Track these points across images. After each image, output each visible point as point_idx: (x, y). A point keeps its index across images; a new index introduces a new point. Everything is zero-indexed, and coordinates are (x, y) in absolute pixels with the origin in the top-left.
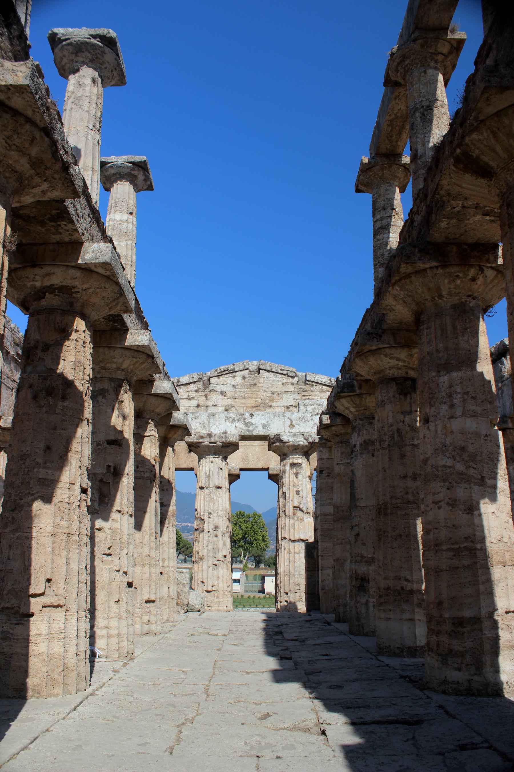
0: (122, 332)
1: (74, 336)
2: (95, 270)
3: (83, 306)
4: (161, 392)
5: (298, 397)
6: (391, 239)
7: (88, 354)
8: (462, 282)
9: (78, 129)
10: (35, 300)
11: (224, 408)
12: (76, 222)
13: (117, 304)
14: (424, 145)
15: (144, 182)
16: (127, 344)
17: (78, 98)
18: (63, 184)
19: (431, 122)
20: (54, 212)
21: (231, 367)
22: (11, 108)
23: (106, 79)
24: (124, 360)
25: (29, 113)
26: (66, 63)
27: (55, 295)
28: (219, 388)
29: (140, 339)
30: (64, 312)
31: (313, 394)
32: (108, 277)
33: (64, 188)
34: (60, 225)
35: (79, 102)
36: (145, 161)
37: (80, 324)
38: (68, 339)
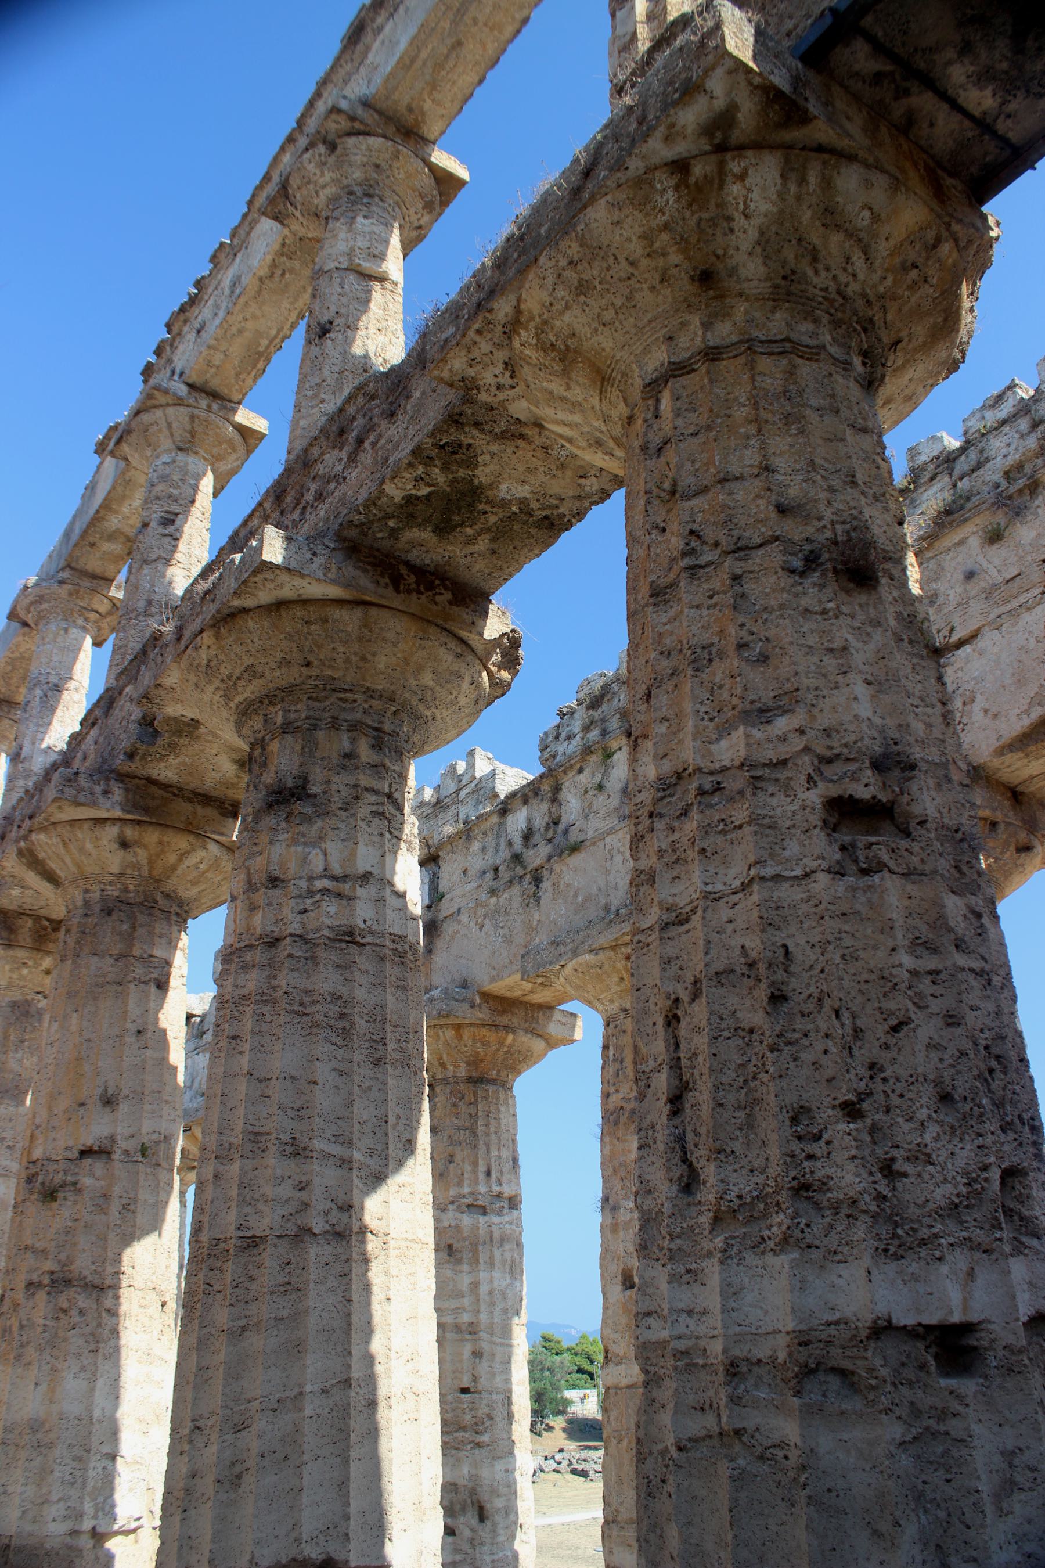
8: (30, 972)
14: (33, 743)
19: (53, 710)
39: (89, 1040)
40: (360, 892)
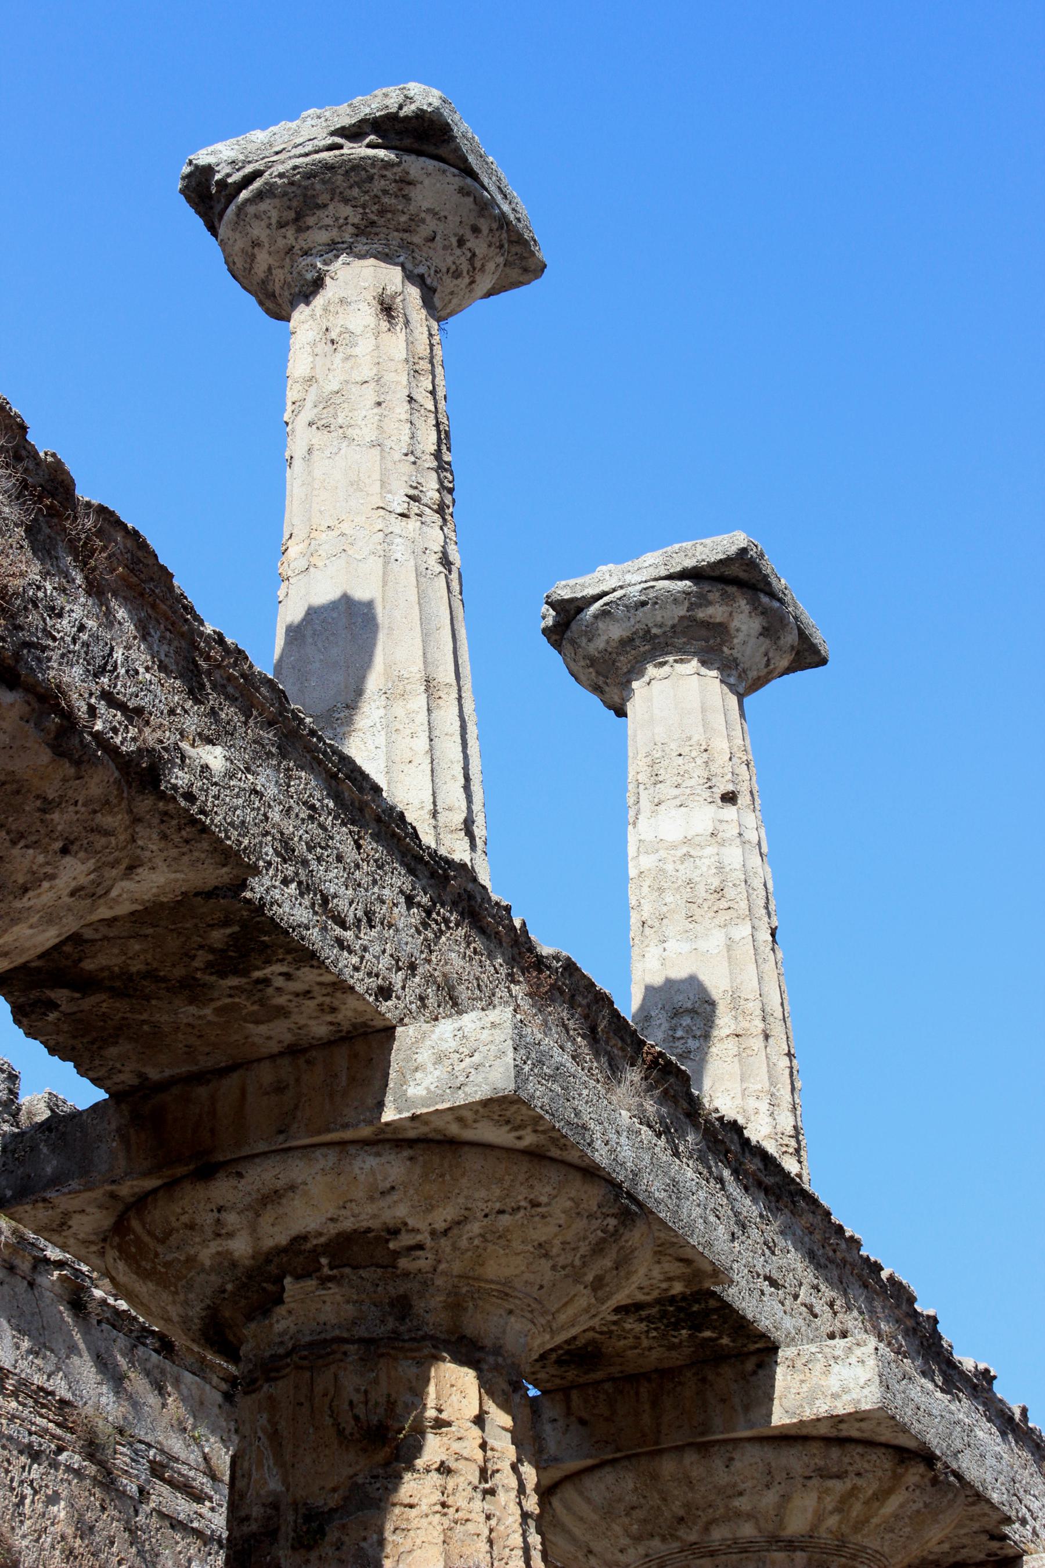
0: (750, 1365)
1: (434, 1449)
2: (469, 1135)
3: (456, 1305)
9: (345, 527)
10: (250, 1318)
12: (329, 953)
13: (622, 1263)
15: (766, 643)
16: (780, 1417)
17: (328, 402)
18: (164, 837)
20: (218, 936)
23: (448, 280)
24: (786, 1498)
26: (270, 269)
27: (324, 1281)
29: (833, 1383)
30: (374, 1350)
32: (535, 1155)
33: (174, 852)
34: (266, 981)
35: (335, 416)
36: (744, 551)
37: (454, 1389)
38: (411, 1467)
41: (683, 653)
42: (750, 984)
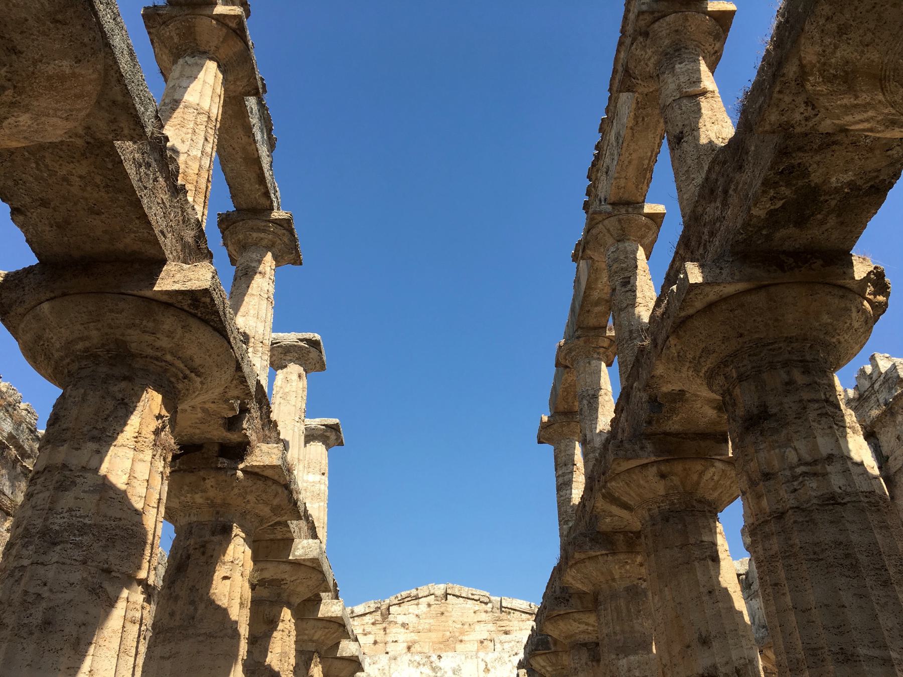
1: (281, 626)
3: (289, 596)
4: (347, 655)
5: (493, 629)
6: (573, 496)
7: (293, 642)
11: (405, 645)
17: (286, 394)
21: (414, 592)
22: (262, 476)
25: (276, 477)
28: (401, 619)
29: (333, 610)
31: (511, 624)
32: (314, 568)
37: (286, 614)
39: (680, 603)
40: (829, 468)
41: (320, 441)
42: (322, 514)
